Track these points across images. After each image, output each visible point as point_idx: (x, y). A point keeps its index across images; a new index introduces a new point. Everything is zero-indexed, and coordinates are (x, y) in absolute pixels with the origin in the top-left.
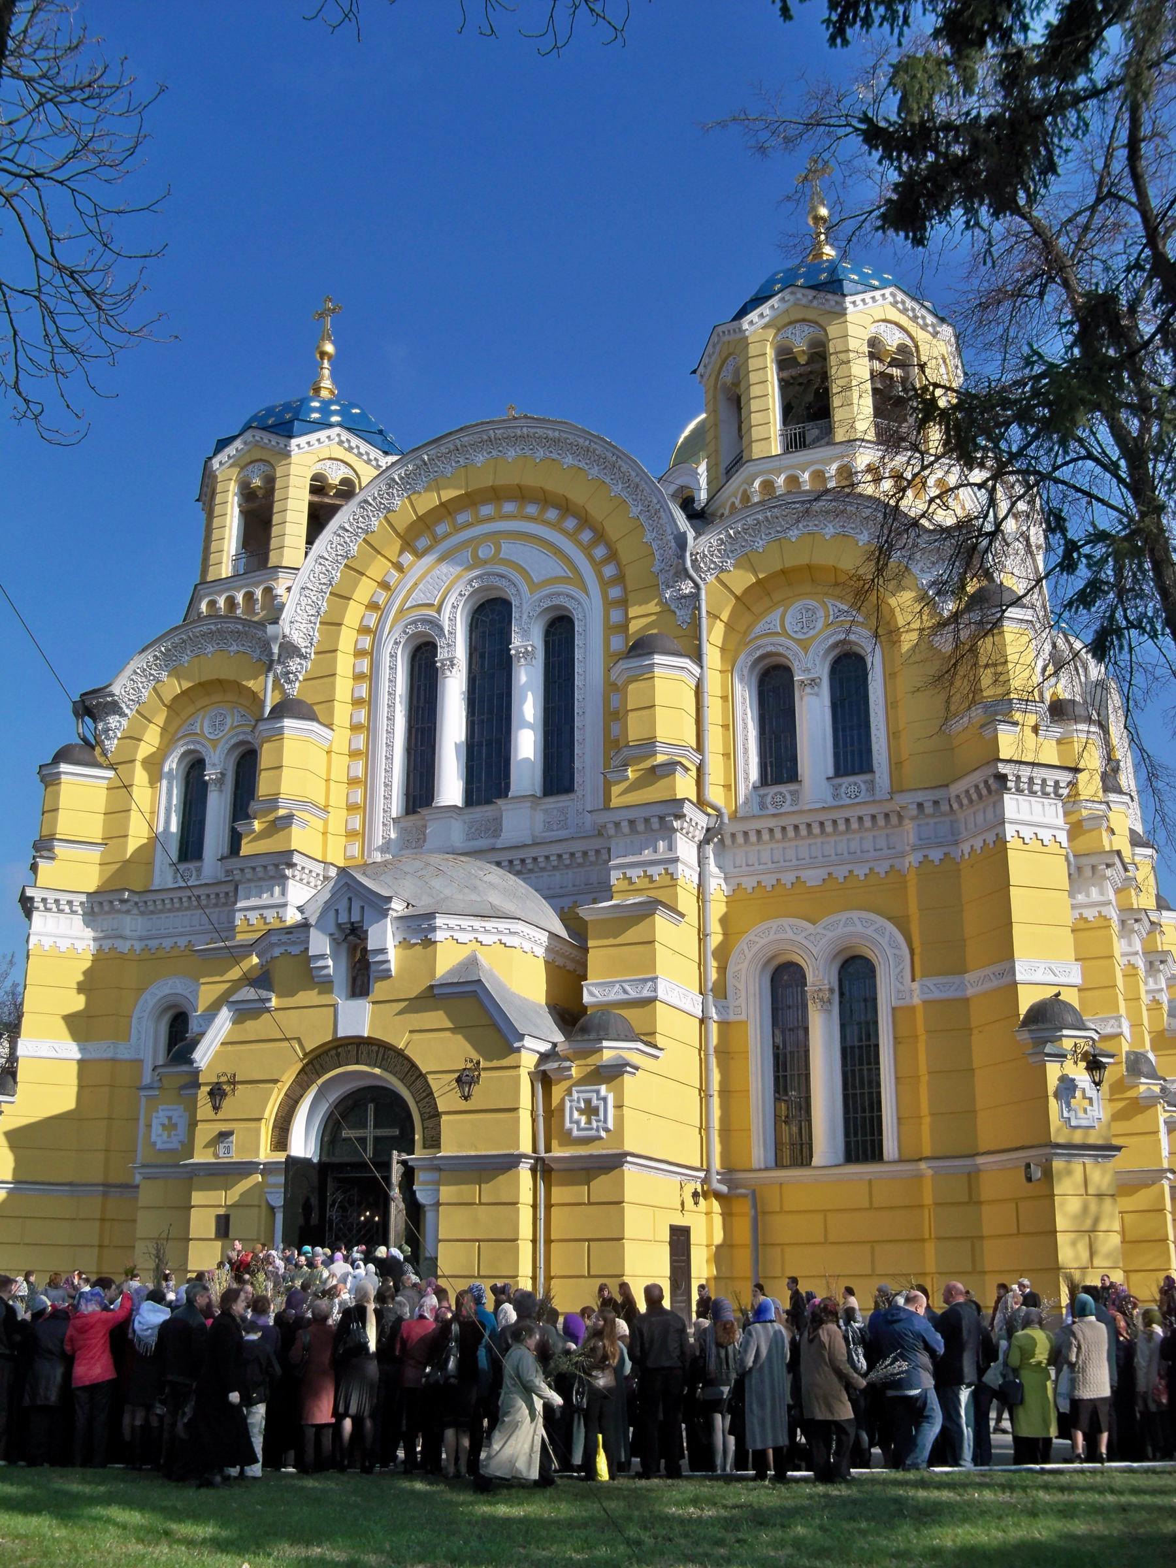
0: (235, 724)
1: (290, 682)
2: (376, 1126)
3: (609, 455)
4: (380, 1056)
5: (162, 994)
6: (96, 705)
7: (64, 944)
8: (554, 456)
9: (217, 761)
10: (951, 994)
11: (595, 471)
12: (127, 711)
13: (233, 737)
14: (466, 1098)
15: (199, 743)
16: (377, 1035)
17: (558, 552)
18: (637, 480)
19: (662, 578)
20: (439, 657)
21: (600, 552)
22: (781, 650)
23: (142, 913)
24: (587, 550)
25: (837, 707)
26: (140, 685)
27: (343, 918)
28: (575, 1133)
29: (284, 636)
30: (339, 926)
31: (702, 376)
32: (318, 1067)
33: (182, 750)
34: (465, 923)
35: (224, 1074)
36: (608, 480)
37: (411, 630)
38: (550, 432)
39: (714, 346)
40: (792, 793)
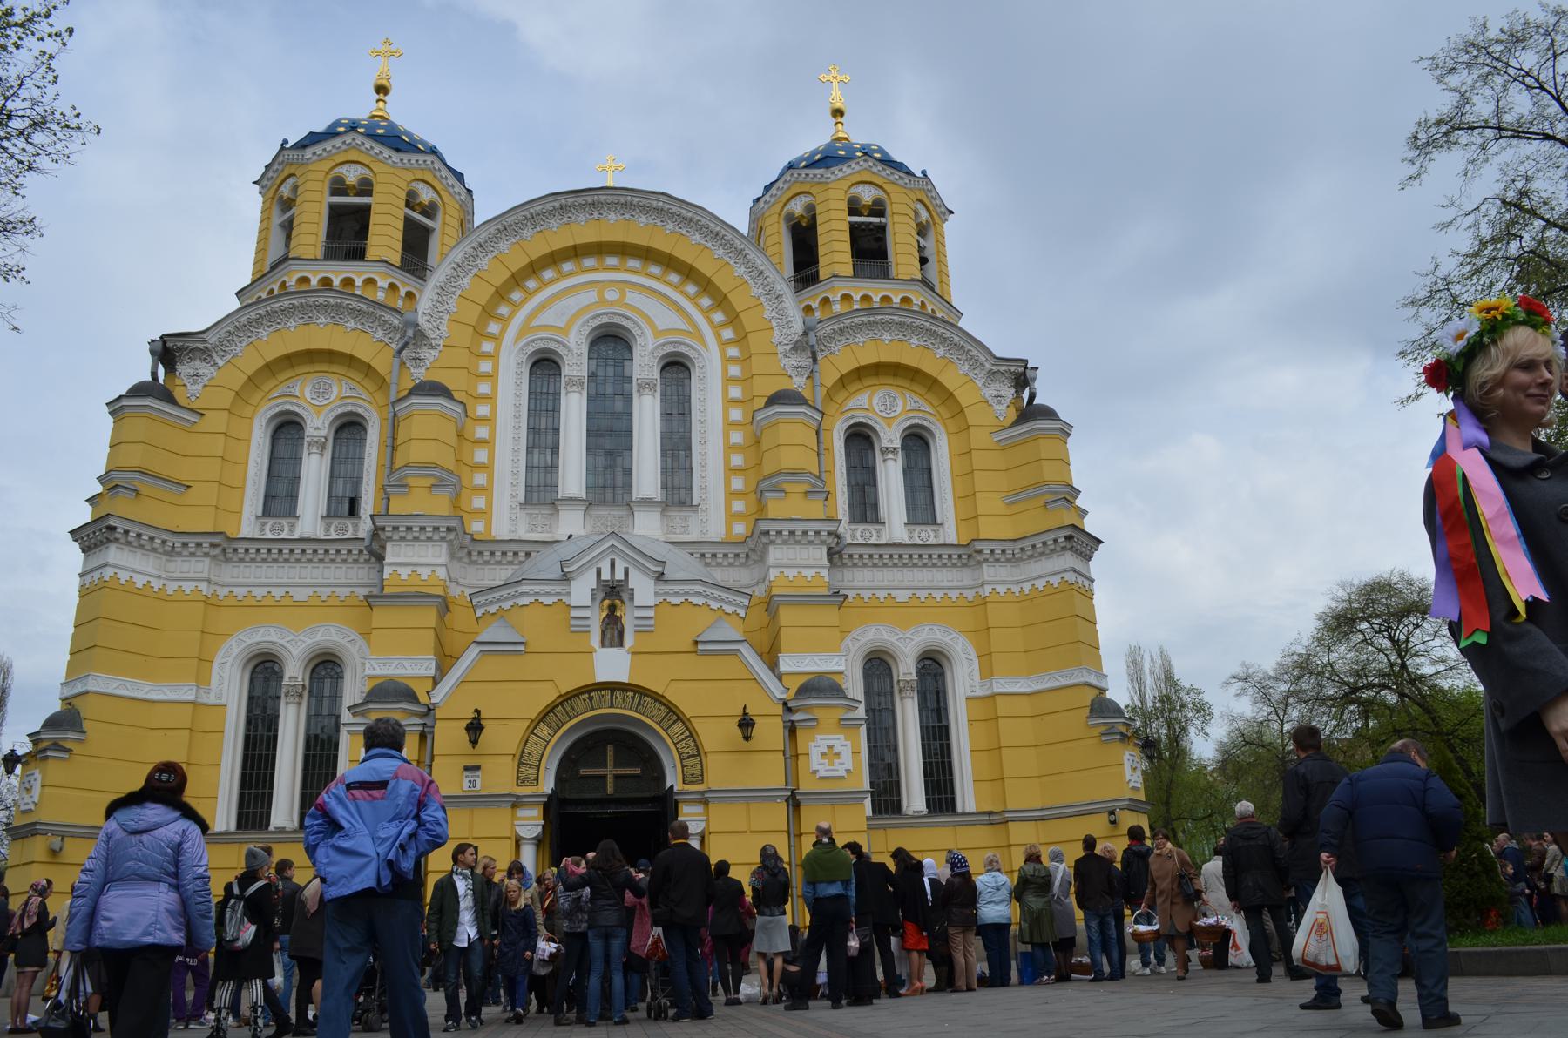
0: (344, 395)
1: (417, 366)
2: (615, 766)
3: (737, 242)
4: (636, 701)
5: (249, 642)
6: (180, 349)
7: (140, 581)
8: (684, 232)
9: (320, 426)
11: (721, 252)
12: (218, 361)
13: (340, 406)
14: (747, 738)
15: (298, 405)
16: (631, 682)
17: (680, 309)
18: (762, 268)
19: (780, 349)
20: (566, 371)
21: (719, 317)
22: (870, 422)
23: (228, 560)
24: (706, 312)
25: (907, 471)
26: (235, 338)
27: (606, 576)
28: (823, 773)
29: (417, 325)
31: (765, 202)
32: (568, 709)
33: (277, 409)
34: (717, 593)
36: (732, 262)
37: (540, 345)
38: (684, 212)
39: (785, 181)
40: (878, 531)
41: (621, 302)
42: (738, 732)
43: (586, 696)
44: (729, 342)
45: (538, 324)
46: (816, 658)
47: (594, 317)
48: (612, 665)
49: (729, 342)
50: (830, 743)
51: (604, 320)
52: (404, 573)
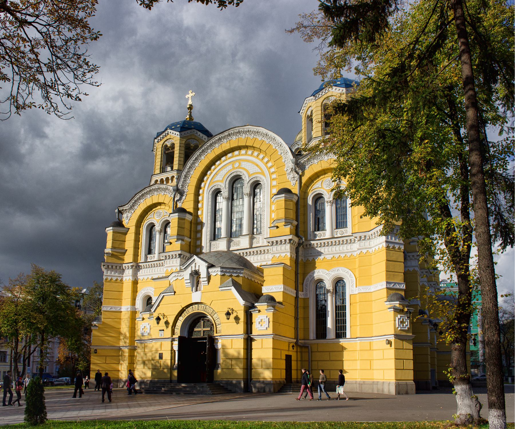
2: (204, 327)
10: (367, 291)
14: (228, 319)
27: (193, 269)
30: (192, 271)
33: (149, 223)
34: (228, 271)
35: (160, 314)
41: (239, 167)
42: (225, 317)
43: (191, 307)
44: (273, 173)
45: (215, 180)
46: (273, 287)
47: (231, 174)
48: (196, 297)
49: (273, 173)
50: (262, 318)
51: (235, 174)
52: (169, 269)
